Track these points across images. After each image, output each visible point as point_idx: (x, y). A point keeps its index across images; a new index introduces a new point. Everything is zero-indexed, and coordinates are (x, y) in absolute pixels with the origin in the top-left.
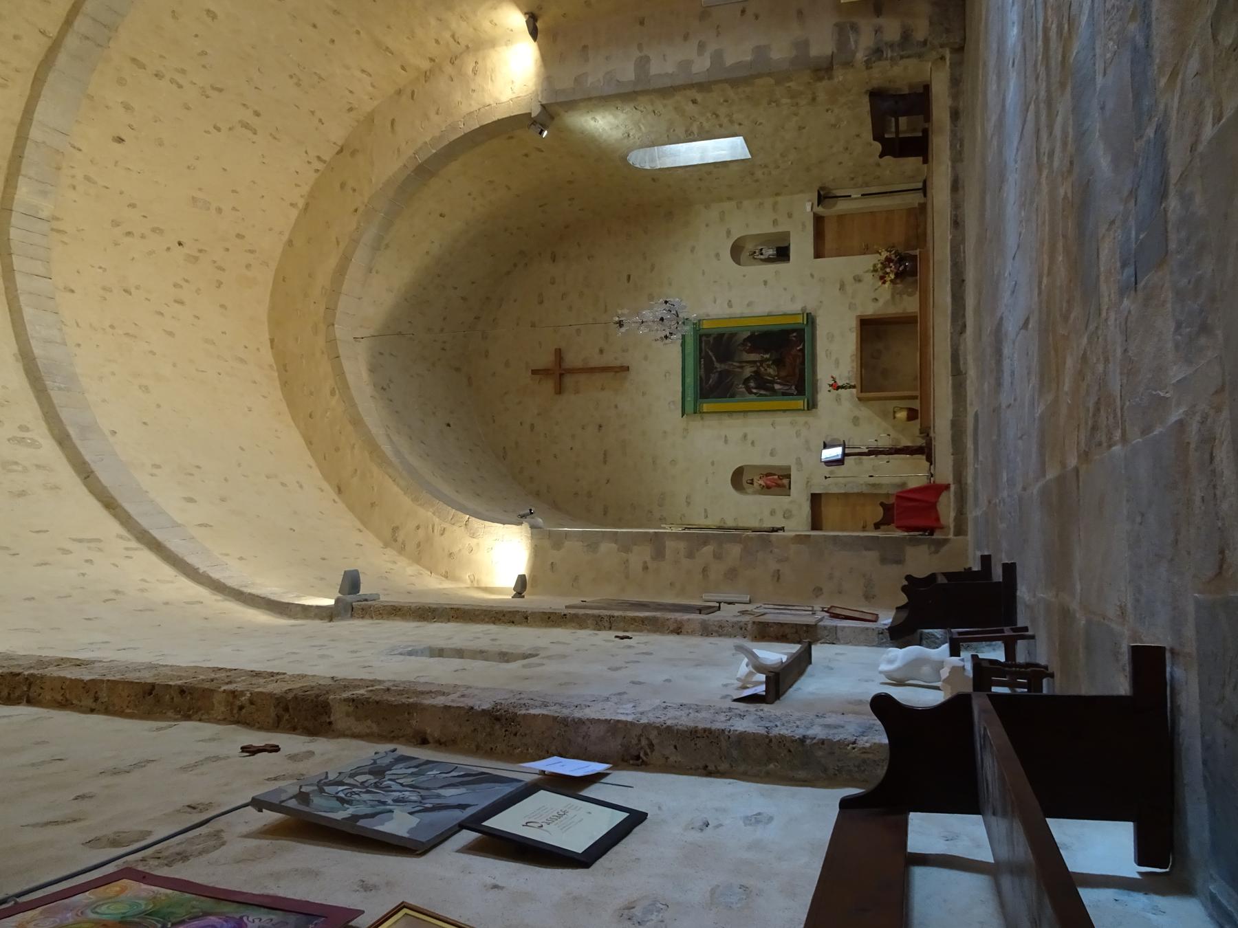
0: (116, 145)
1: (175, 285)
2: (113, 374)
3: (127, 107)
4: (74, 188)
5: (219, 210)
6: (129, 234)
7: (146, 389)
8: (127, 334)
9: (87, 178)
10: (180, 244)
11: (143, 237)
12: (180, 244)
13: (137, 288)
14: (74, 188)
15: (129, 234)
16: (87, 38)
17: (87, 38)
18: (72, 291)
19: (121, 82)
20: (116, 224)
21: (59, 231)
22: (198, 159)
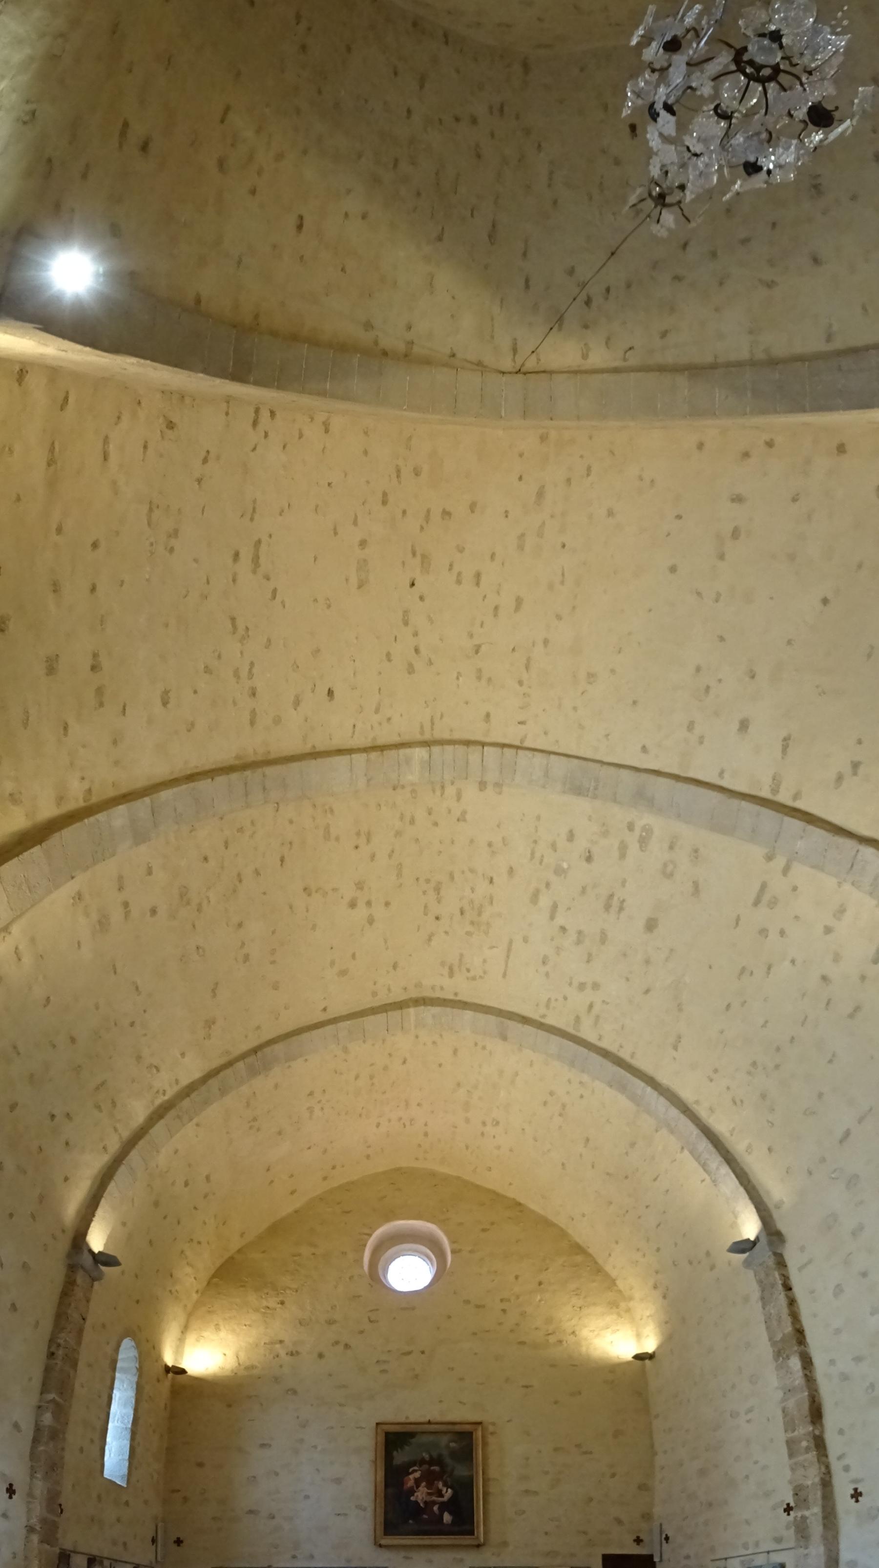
0: (336, 694)
1: (459, 582)
2: (575, 709)
3: (297, 703)
4: (389, 719)
5: (363, 544)
6: (417, 651)
7: (591, 677)
8: (527, 667)
9: (377, 711)
10: (413, 585)
11: (416, 634)
12: (413, 585)
13: (471, 636)
14: (389, 719)
15: (417, 651)
16: (264, 789)
17: (264, 789)
18: (488, 715)
19: (277, 721)
20: (411, 669)
21: (433, 723)
22: (316, 600)
